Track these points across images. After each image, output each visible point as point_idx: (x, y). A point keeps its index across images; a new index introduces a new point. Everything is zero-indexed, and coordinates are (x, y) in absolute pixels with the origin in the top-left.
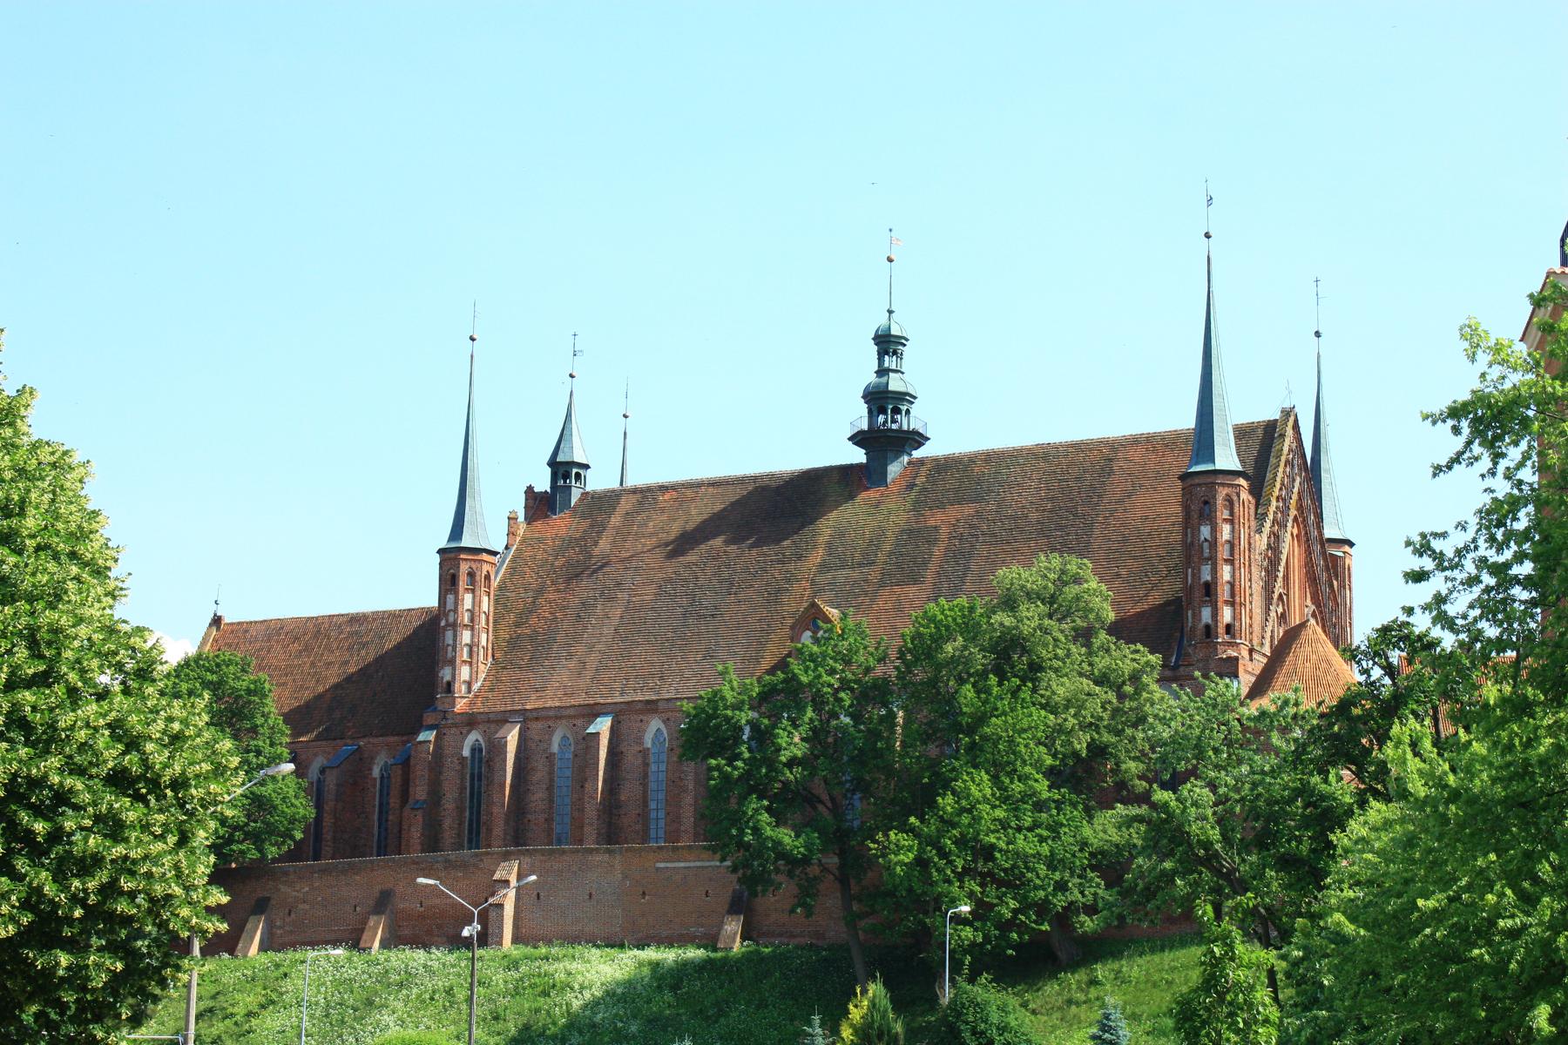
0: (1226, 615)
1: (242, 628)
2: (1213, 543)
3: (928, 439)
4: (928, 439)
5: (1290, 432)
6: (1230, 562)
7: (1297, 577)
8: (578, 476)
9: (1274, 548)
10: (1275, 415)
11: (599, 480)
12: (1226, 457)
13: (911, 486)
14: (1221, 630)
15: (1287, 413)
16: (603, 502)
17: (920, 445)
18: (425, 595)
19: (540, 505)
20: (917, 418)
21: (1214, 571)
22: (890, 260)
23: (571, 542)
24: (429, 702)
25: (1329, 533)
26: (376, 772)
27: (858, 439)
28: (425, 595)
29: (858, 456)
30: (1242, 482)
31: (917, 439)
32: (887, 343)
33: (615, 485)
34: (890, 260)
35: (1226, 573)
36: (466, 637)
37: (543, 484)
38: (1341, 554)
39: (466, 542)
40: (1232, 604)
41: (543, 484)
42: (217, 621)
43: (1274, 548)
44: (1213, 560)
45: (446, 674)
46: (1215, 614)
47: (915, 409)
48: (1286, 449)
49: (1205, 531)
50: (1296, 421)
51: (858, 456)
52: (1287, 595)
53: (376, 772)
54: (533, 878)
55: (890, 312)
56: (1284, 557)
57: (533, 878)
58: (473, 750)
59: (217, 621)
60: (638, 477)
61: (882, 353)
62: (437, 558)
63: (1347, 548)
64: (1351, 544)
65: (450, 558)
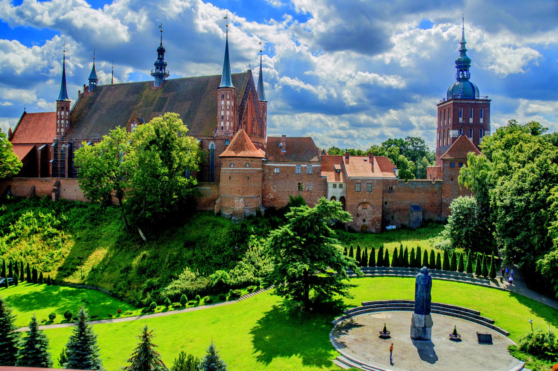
3: (169, 75)
4: (169, 75)
17: (167, 77)
23: (91, 98)
27: (153, 75)
33: (111, 83)
47: (167, 68)
51: (153, 79)
55: (161, 44)
56: (246, 107)
59: (25, 113)
61: (159, 55)
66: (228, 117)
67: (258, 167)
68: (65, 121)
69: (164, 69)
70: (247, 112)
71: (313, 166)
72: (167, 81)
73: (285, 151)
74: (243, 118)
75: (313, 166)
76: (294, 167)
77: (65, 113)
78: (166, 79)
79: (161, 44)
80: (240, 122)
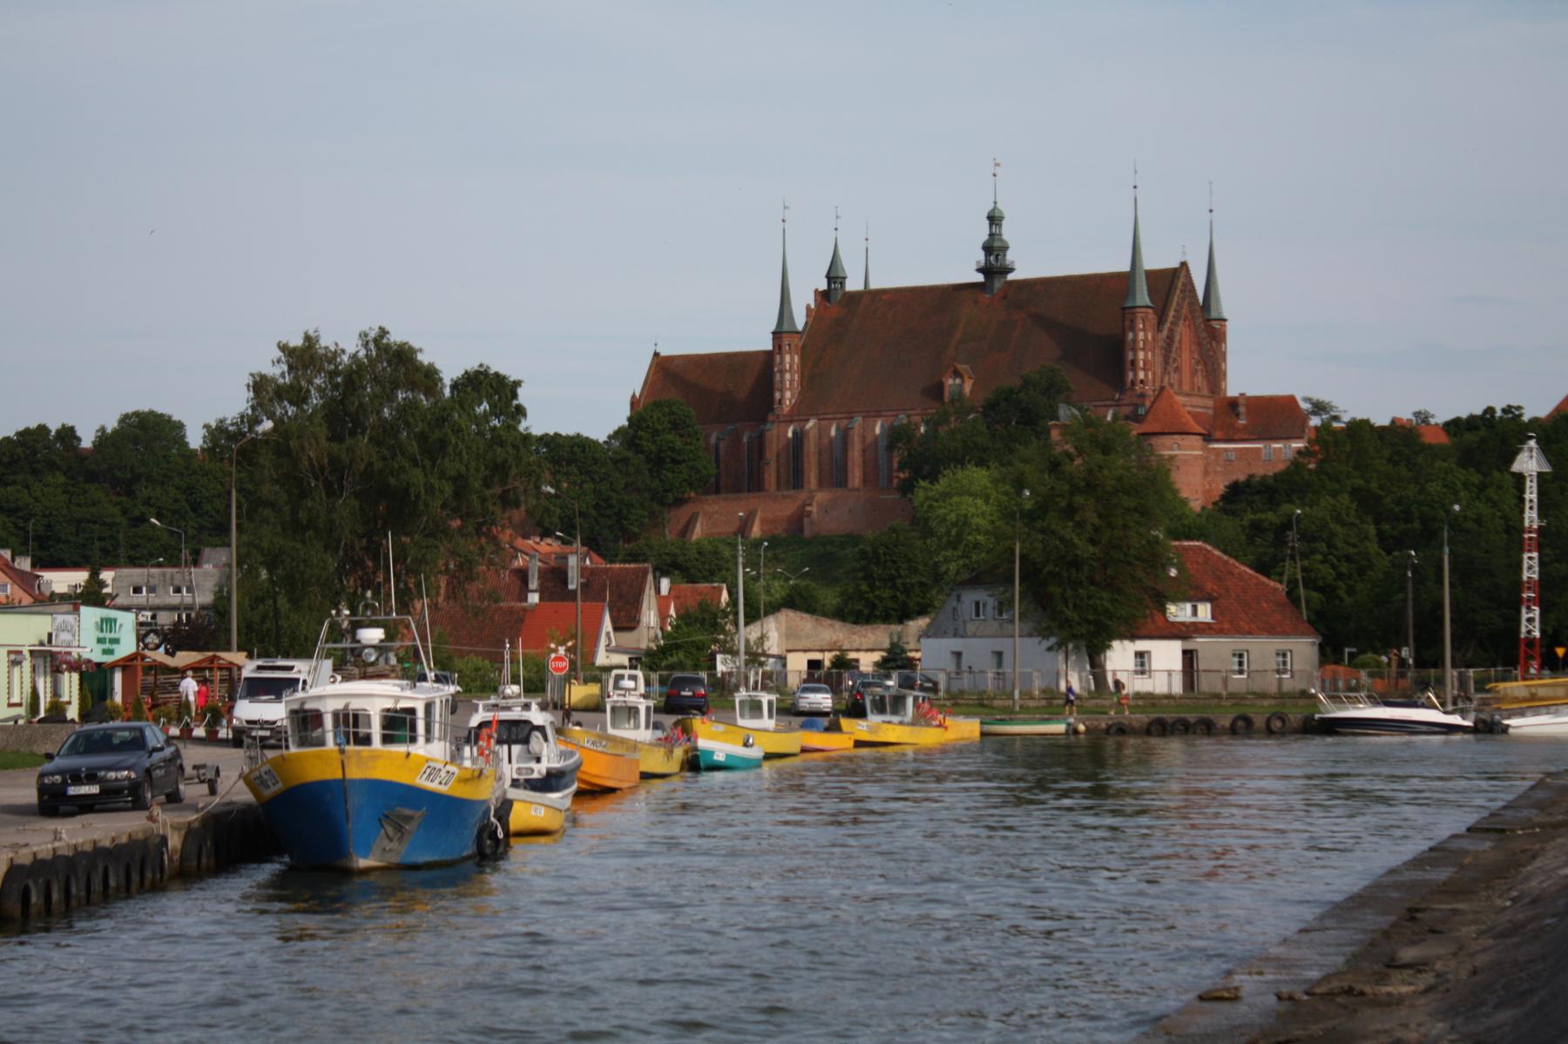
0: (1141, 375)
1: (670, 359)
2: (1135, 341)
5: (1183, 273)
6: (1143, 349)
7: (1186, 347)
8: (841, 283)
9: (1170, 338)
10: (1175, 264)
11: (853, 284)
12: (1142, 297)
13: (1005, 297)
14: (1138, 382)
15: (1184, 265)
16: (854, 297)
18: (767, 345)
19: (823, 296)
20: (1011, 256)
21: (1135, 354)
22: (994, 175)
24: (771, 409)
25: (1214, 315)
26: (745, 440)
27: (979, 270)
28: (767, 345)
29: (980, 278)
30: (1150, 311)
31: (1011, 270)
32: (994, 219)
34: (994, 175)
35: (1141, 355)
36: (788, 376)
37: (823, 286)
38: (1218, 327)
39: (786, 328)
40: (1144, 369)
41: (823, 286)
42: (656, 355)
43: (1170, 338)
44: (1134, 350)
45: (777, 395)
46: (1136, 374)
48: (1180, 285)
49: (1130, 336)
50: (1188, 271)
51: (980, 278)
52: (1180, 356)
53: (745, 440)
54: (807, 569)
55: (995, 203)
56: (1177, 338)
57: (807, 569)
58: (793, 433)
59: (656, 355)
60: (875, 284)
62: (771, 336)
63: (1223, 323)
64: (1225, 320)
65: (777, 335)
66: (1141, 362)
67: (1192, 448)
68: (792, 376)
69: (1005, 255)
70: (1181, 348)
71: (1294, 445)
72: (1012, 282)
73: (1244, 422)
74: (1171, 360)
75: (1294, 445)
76: (1259, 449)
77: (792, 359)
78: (1010, 277)
79: (995, 203)
80: (1166, 368)
